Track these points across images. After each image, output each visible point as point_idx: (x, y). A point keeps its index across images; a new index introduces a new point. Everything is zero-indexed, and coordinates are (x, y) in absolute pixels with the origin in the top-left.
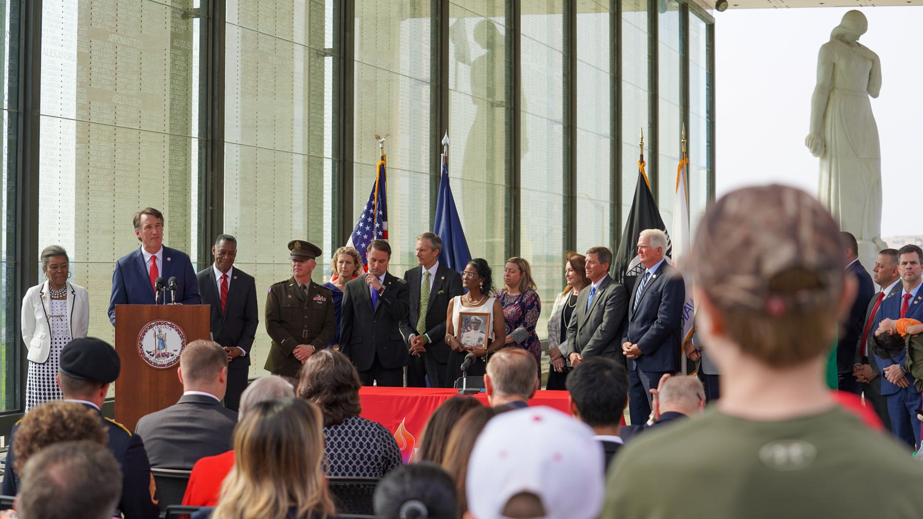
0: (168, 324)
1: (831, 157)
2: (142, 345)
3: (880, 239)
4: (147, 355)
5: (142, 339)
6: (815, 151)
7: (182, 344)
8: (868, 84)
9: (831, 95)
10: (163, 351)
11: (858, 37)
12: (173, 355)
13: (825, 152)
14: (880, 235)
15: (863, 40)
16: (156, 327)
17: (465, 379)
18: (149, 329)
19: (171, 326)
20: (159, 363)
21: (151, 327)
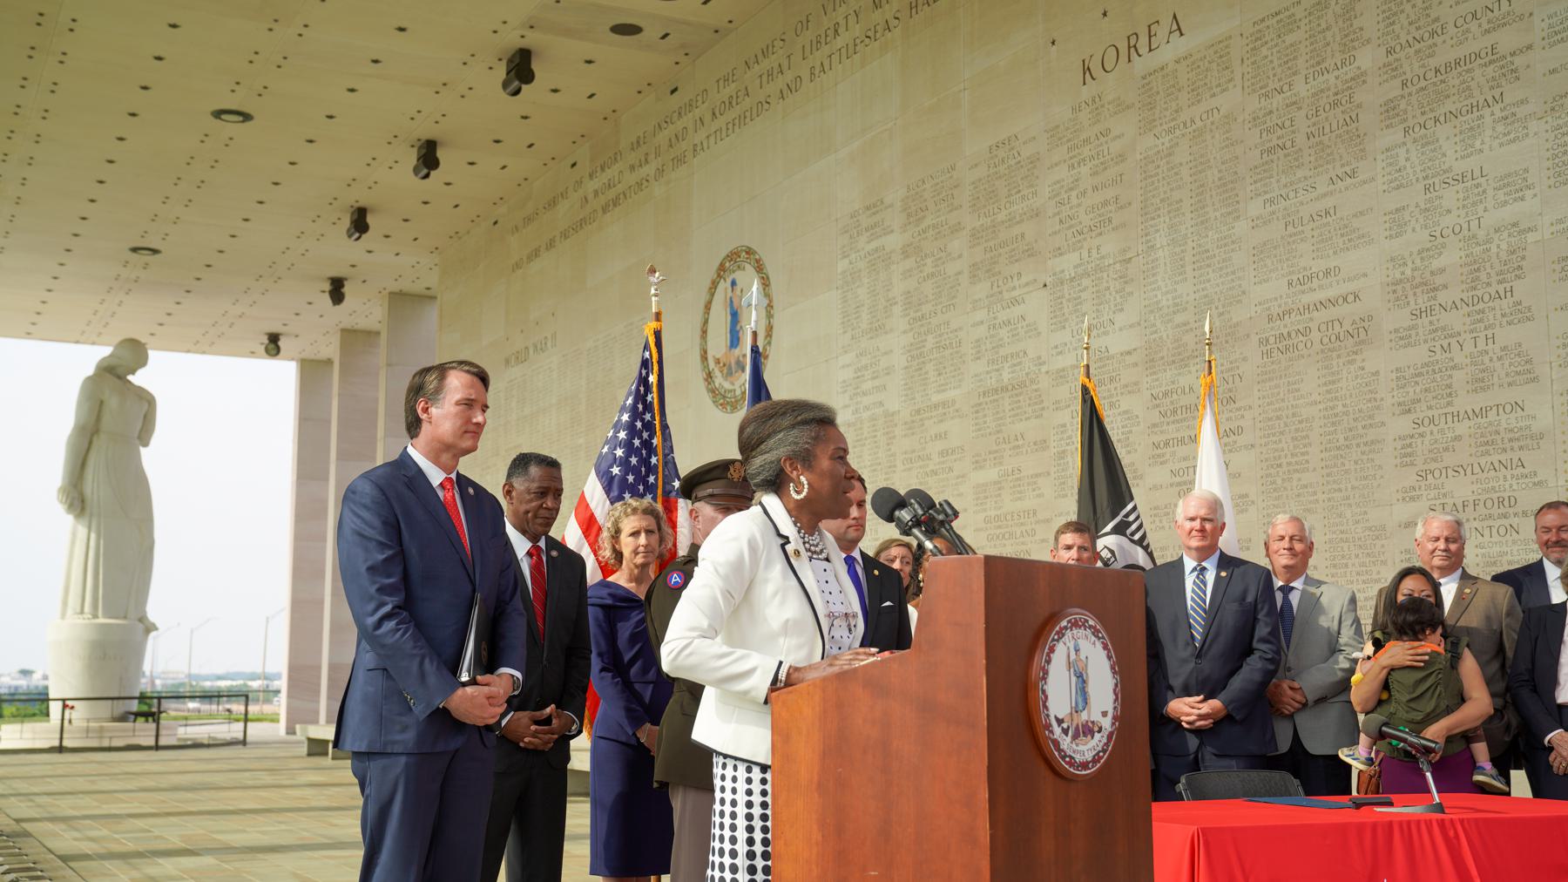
0: (1090, 627)
1: (91, 515)
2: (1046, 697)
3: (147, 618)
4: (1057, 730)
5: (1046, 673)
6: (71, 507)
7: (1114, 690)
8: (141, 431)
9: (95, 439)
10: (1084, 716)
11: (133, 373)
12: (1099, 731)
13: (83, 509)
14: (145, 612)
15: (137, 379)
16: (1070, 635)
17: (1428, 775)
18: (1058, 641)
19: (1096, 632)
20: (1078, 758)
21: (1061, 634)
